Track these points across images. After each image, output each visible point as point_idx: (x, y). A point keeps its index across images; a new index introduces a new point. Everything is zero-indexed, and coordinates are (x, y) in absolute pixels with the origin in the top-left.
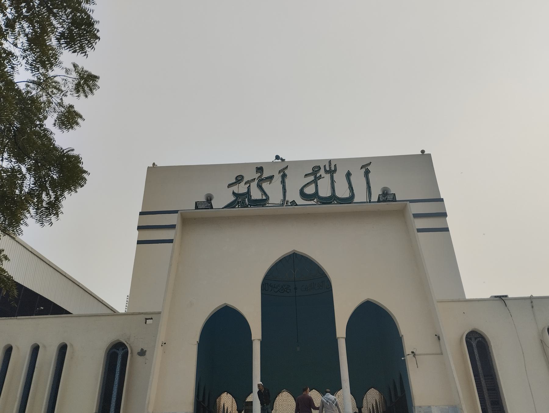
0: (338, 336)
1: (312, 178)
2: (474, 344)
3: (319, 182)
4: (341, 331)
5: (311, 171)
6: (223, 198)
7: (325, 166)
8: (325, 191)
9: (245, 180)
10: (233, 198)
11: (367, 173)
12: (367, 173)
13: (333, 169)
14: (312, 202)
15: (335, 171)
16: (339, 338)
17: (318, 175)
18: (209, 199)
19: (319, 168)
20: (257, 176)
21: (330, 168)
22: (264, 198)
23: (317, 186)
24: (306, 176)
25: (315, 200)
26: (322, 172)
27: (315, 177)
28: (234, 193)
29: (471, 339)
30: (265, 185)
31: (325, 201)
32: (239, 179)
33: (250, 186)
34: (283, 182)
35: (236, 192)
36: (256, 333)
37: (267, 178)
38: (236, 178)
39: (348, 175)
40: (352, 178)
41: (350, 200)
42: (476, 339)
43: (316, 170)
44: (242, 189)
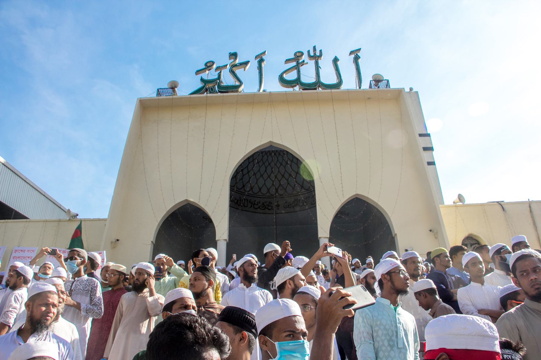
0: (319, 236)
1: (294, 64)
3: (302, 69)
5: (293, 57)
7: (309, 52)
10: (200, 85)
11: (356, 59)
12: (357, 58)
13: (318, 54)
16: (320, 238)
18: (173, 87)
19: (302, 54)
20: (229, 62)
21: (315, 54)
22: (237, 83)
23: (299, 72)
24: (288, 61)
25: (297, 88)
26: (305, 58)
27: (298, 64)
28: (202, 80)
30: (239, 72)
32: (209, 66)
33: (221, 72)
34: (260, 68)
35: (205, 78)
38: (206, 65)
39: (336, 60)
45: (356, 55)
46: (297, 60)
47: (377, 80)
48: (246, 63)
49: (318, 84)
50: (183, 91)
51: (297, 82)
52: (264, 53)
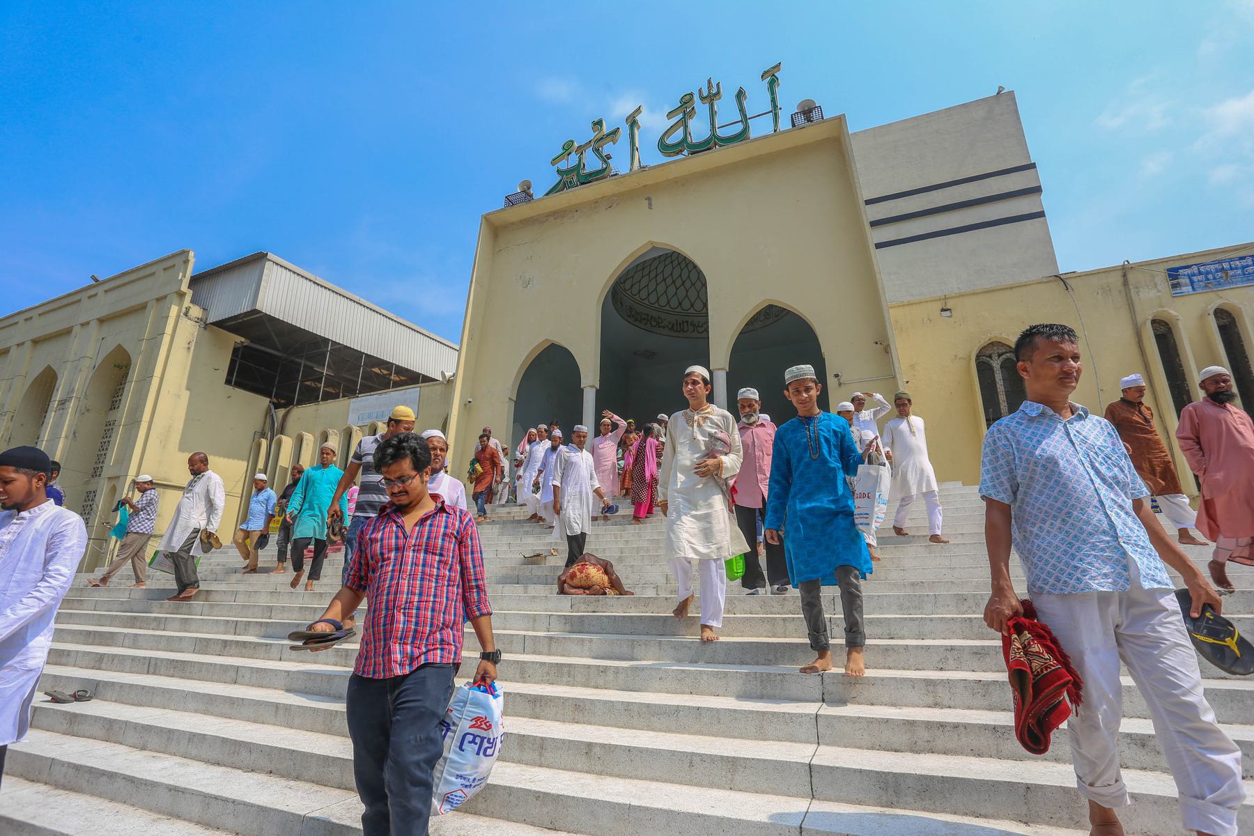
1: (681, 116)
2: (996, 364)
3: (692, 123)
9: (576, 145)
13: (714, 91)
14: (680, 157)
15: (718, 92)
20: (592, 135)
23: (686, 127)
25: (685, 152)
30: (607, 149)
32: (568, 148)
36: (590, 378)
39: (740, 95)
41: (742, 136)
42: (999, 356)
44: (573, 160)
45: (771, 77)
46: (685, 108)
47: (808, 111)
48: (616, 131)
50: (538, 192)
52: (638, 110)
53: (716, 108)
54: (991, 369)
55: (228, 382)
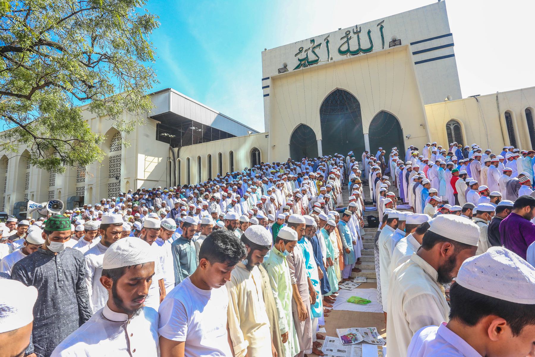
1: (345, 39)
2: (452, 127)
3: (350, 41)
4: (366, 131)
6: (293, 63)
8: (354, 47)
12: (382, 28)
13: (359, 30)
15: (360, 31)
17: (349, 37)
18: (285, 66)
20: (311, 45)
23: (348, 44)
26: (352, 34)
27: (348, 39)
28: (299, 59)
29: (450, 125)
30: (317, 50)
31: (355, 53)
32: (301, 50)
34: (327, 47)
35: (300, 58)
36: (319, 137)
37: (317, 46)
39: (369, 32)
40: (371, 34)
43: (348, 33)
44: (303, 56)
48: (320, 45)
49: (360, 50)
50: (291, 68)
51: (348, 51)
53: (360, 37)
54: (450, 129)
55: (157, 139)
